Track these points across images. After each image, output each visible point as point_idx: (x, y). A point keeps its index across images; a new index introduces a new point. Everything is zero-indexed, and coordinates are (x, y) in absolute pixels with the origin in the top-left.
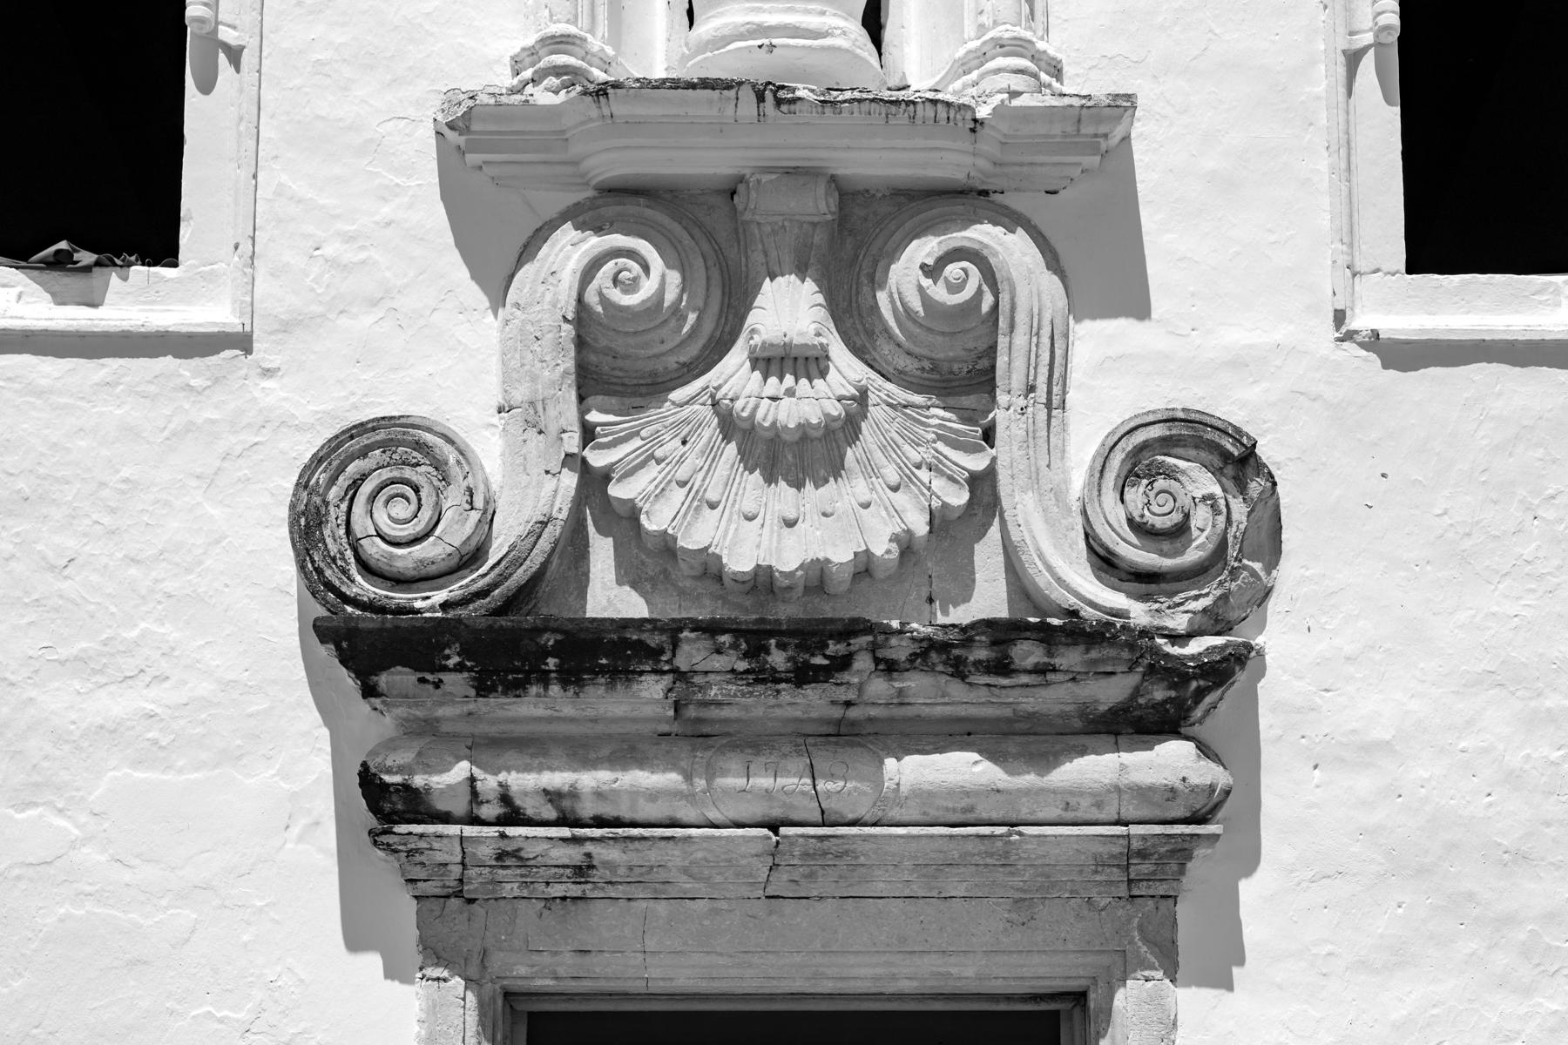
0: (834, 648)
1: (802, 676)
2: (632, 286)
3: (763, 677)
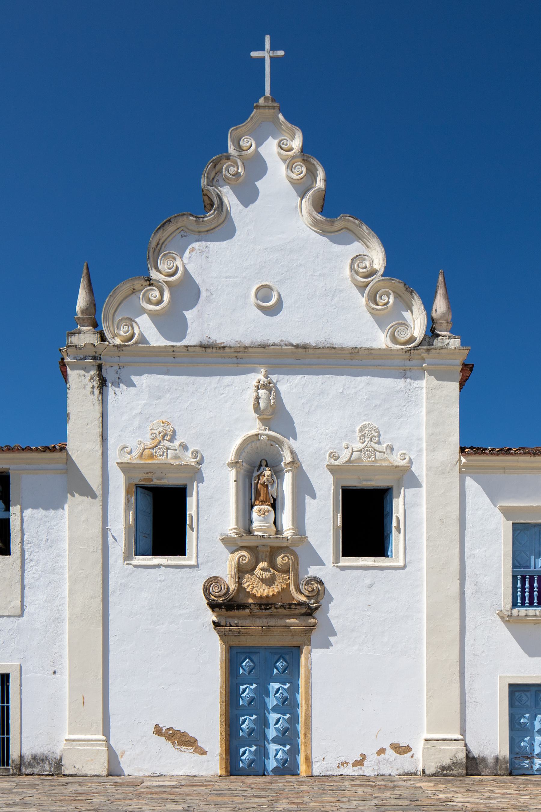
0: (270, 606)
1: (266, 609)
2: (245, 560)
3: (261, 609)
